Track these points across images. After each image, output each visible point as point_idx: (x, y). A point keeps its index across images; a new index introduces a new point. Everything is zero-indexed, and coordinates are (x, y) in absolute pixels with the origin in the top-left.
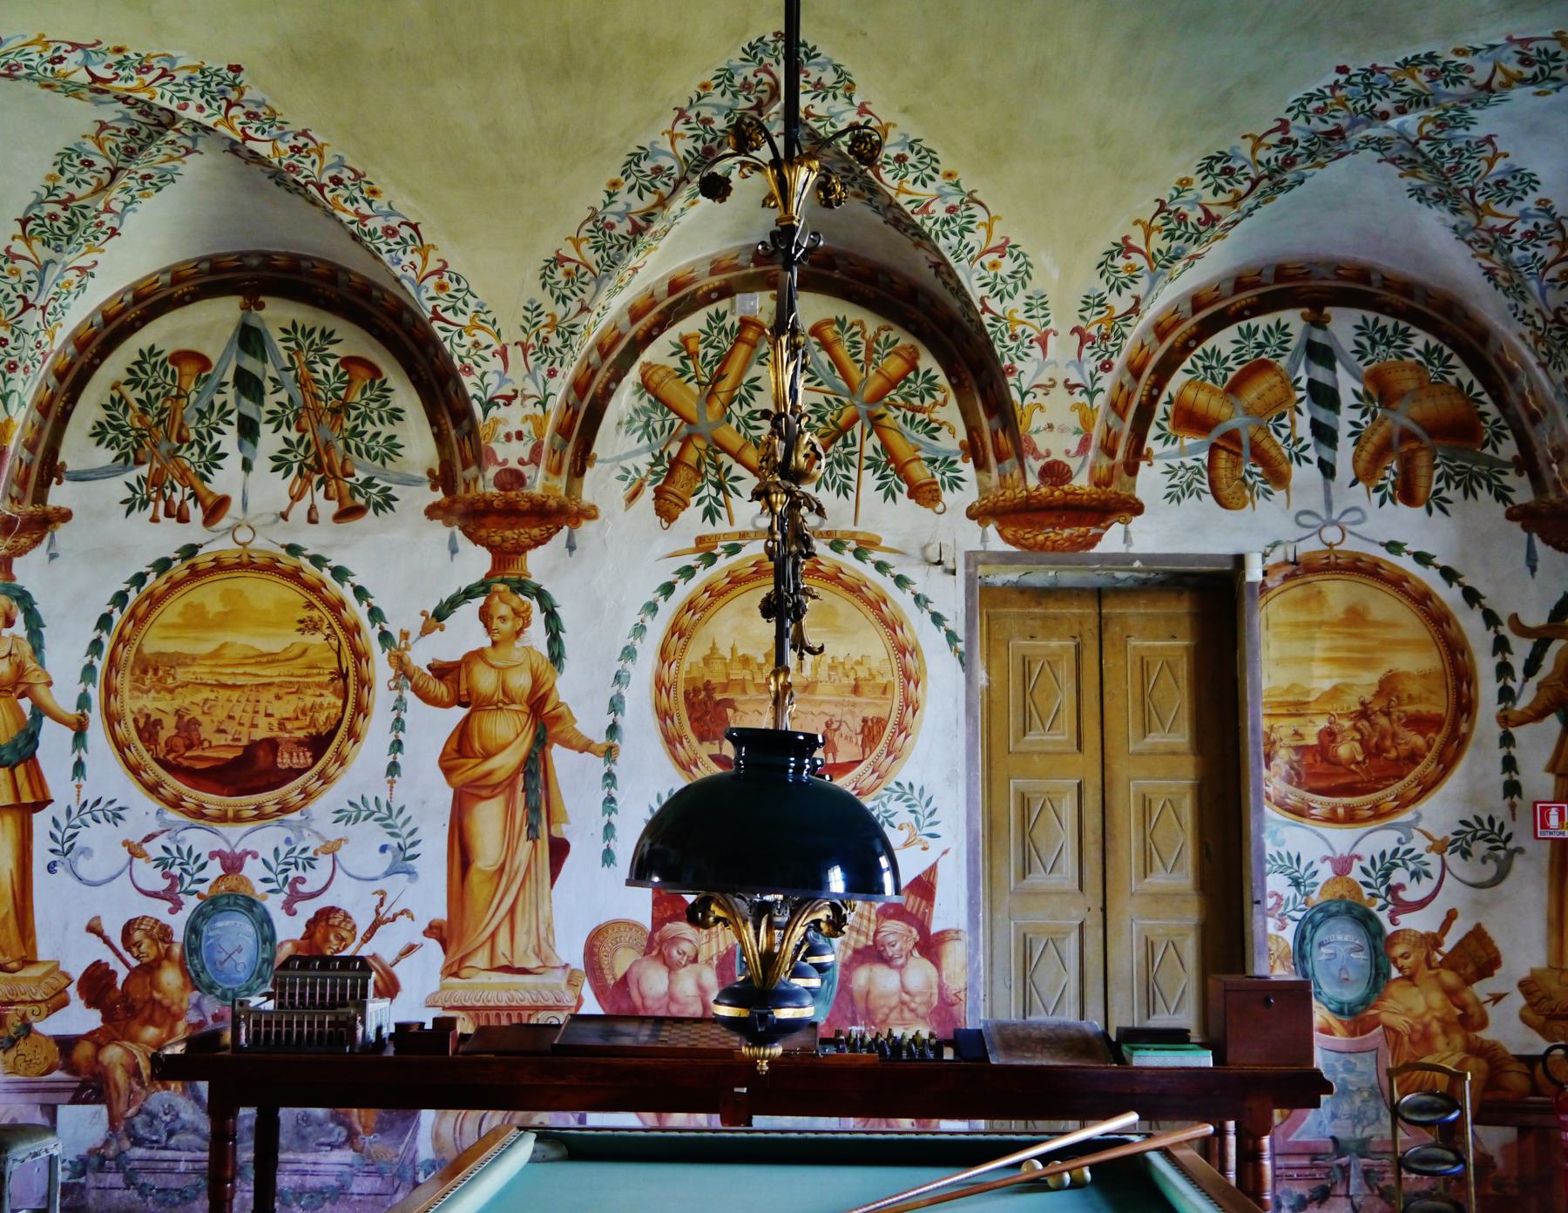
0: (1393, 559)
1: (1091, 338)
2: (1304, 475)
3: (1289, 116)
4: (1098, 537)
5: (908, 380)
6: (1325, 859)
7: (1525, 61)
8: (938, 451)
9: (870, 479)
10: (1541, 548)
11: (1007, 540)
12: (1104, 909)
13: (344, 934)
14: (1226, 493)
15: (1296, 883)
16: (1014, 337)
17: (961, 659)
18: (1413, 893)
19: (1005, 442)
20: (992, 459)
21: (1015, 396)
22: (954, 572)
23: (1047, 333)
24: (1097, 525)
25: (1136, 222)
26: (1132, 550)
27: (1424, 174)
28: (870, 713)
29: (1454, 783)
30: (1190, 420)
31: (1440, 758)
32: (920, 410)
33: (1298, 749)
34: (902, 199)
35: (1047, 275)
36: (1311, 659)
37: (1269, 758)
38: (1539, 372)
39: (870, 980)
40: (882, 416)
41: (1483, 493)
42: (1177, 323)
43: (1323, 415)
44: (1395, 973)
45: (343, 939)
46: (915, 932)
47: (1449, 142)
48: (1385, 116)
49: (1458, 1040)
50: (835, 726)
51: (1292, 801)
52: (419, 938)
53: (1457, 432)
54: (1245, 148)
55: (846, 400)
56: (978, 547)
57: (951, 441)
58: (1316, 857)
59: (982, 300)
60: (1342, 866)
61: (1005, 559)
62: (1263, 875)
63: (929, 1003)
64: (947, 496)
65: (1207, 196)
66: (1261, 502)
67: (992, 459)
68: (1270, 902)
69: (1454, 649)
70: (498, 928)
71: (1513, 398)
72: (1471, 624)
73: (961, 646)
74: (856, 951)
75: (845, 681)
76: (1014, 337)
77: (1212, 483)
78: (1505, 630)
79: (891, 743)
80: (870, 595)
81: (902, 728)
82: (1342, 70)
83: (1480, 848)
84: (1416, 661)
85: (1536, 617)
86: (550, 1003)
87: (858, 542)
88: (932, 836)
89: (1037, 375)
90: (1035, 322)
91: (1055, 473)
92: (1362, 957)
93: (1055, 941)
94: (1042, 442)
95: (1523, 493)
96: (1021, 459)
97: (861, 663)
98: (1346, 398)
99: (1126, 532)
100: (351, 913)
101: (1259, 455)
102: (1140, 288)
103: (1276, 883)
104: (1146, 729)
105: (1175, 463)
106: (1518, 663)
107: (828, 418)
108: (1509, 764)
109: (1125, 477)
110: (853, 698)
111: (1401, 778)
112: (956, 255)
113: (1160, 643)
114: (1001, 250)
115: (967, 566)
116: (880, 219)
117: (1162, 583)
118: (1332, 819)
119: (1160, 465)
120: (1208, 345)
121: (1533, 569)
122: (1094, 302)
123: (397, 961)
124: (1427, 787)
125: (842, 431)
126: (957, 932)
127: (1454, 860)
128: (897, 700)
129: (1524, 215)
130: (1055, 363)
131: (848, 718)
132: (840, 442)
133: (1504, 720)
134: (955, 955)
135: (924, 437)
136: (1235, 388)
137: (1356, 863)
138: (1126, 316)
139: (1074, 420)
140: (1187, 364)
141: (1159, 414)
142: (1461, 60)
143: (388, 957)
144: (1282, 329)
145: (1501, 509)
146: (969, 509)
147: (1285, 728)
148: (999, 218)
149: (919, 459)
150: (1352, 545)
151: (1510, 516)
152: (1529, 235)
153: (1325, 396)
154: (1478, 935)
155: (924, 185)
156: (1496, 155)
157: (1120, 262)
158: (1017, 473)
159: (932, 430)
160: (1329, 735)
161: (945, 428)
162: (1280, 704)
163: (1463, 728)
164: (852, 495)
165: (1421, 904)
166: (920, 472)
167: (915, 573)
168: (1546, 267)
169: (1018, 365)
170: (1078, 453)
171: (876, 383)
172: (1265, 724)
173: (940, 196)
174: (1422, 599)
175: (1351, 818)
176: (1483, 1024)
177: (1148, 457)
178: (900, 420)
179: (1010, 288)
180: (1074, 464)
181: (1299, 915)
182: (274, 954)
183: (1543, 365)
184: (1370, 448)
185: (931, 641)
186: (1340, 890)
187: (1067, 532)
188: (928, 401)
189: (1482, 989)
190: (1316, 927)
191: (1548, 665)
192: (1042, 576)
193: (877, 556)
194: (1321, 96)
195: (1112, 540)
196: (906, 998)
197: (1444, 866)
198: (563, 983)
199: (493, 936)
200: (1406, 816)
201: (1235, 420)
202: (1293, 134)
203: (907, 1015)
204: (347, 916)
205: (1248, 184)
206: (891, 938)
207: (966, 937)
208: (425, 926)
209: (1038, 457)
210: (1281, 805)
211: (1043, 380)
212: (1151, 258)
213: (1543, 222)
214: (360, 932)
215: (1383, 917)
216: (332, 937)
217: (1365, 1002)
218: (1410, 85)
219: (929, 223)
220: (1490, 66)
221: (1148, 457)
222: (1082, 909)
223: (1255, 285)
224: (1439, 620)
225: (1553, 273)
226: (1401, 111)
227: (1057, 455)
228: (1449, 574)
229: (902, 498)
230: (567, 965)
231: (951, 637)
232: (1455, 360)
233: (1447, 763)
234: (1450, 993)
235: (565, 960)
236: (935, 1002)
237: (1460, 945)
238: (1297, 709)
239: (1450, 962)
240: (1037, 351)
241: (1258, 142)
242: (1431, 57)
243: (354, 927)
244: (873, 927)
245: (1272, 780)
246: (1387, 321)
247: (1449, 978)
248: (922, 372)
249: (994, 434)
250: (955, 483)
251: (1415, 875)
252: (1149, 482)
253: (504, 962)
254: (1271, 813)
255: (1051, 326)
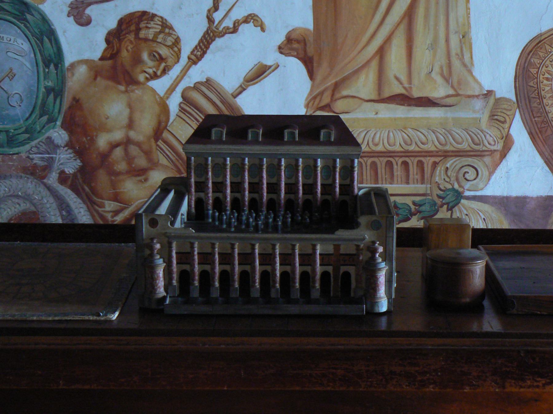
13: (164, 51)
45: (161, 59)
52: (272, 57)
70: (388, 39)
86: (464, 146)
100: (171, 21)
123: (242, 89)
143: (229, 83)
182: (63, 82)
198: (485, 118)
199: (381, 52)
204: (165, 26)
208: (281, 38)
214: (187, 49)
216: (145, 56)
230: (490, 93)
235: (487, 86)
243: (177, 41)
253: (398, 89)
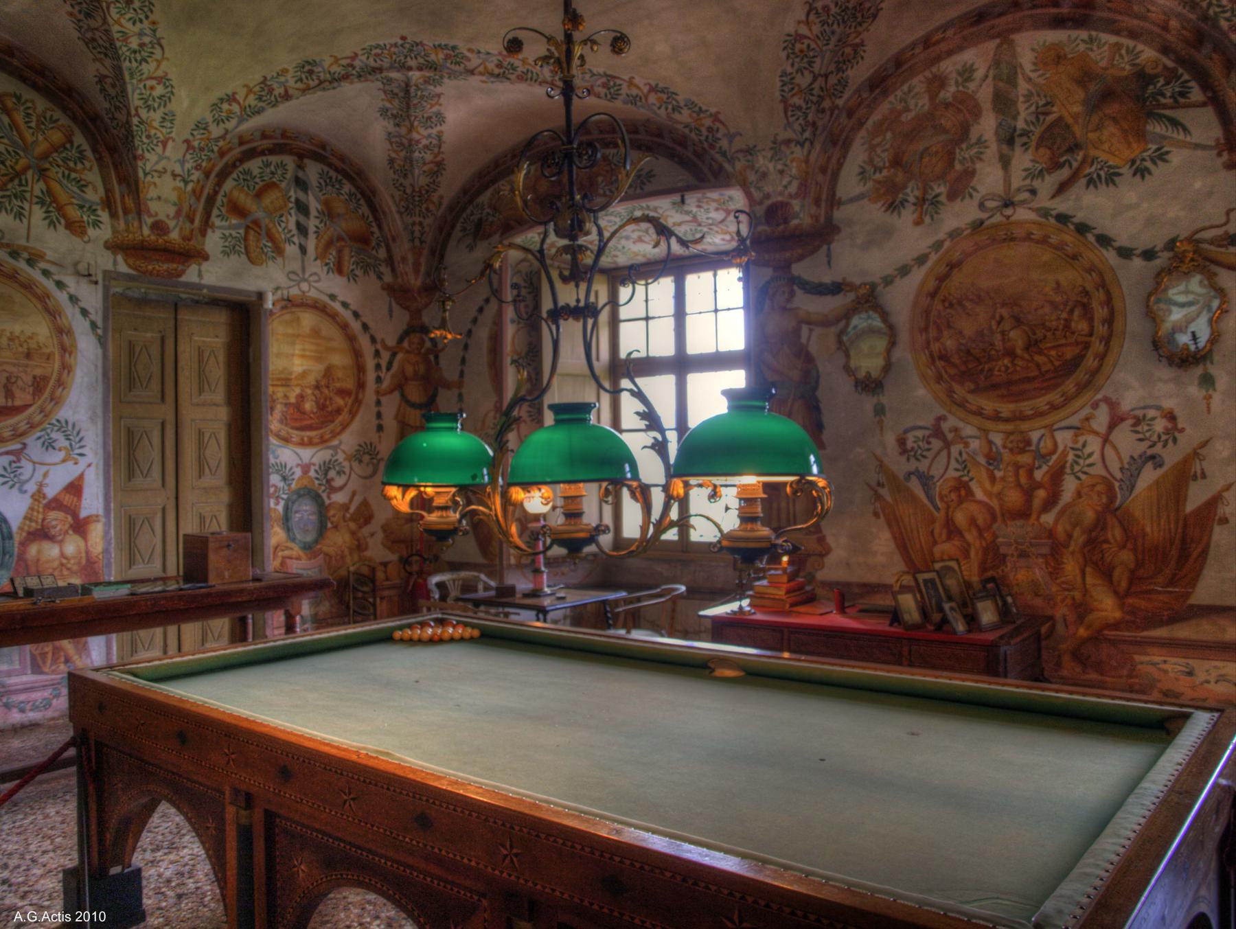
0: (332, 304)
1: (194, 148)
2: (291, 250)
3: (360, 53)
4: (183, 272)
5: (66, 149)
6: (298, 465)
7: (499, 65)
8: (84, 200)
9: (38, 213)
10: (396, 307)
11: (130, 266)
12: (177, 498)
14: (253, 255)
15: (284, 479)
16: (148, 137)
17: (99, 341)
18: (338, 482)
19: (130, 202)
20: (120, 212)
21: (141, 174)
22: (96, 283)
23: (168, 139)
24: (183, 263)
25: (246, 86)
26: (203, 282)
27: (396, 102)
28: (38, 372)
29: (356, 425)
30: (237, 210)
31: (350, 412)
32: (75, 171)
33: (286, 405)
34: (116, 28)
35: (182, 102)
36: (293, 355)
37: (272, 409)
38: (397, 216)
39: (39, 552)
40: (46, 170)
41: (372, 274)
42: (230, 149)
43: (302, 219)
44: (329, 525)
46: (70, 518)
47: (423, 90)
48: (410, 69)
49: (356, 557)
50: (13, 380)
51: (283, 433)
53: (362, 240)
54: (327, 61)
55: (21, 153)
56: (110, 267)
57: (94, 195)
58: (294, 464)
59: (136, 110)
60: (306, 468)
61: (129, 278)
62: (269, 474)
63: (79, 563)
64: (91, 232)
65: (291, 83)
66: (270, 263)
67: (120, 212)
68: (272, 490)
69: (357, 354)
71: (386, 228)
72: (364, 342)
73: (100, 332)
74: (29, 533)
75: (20, 349)
76: (148, 137)
77: (246, 248)
78: (379, 346)
79: (53, 393)
80: (39, 292)
81: (60, 383)
82: (403, 38)
83: (366, 458)
84: (340, 360)
85: (391, 341)
87: (30, 254)
88: (82, 455)
89: (157, 163)
90: (164, 130)
91: (159, 227)
92: (313, 518)
93: (149, 520)
94: (154, 206)
95: (388, 278)
96: (139, 213)
97: (31, 338)
98: (313, 212)
99: (200, 271)
101: (270, 237)
102: (230, 125)
103: (275, 479)
104: (201, 391)
105: (227, 232)
106: (384, 364)
107: (8, 163)
108: (379, 415)
109: (200, 238)
110: (26, 362)
111: (333, 421)
112: (131, 75)
113: (208, 337)
114: (160, 80)
115: (104, 280)
116: (76, 34)
117: (206, 303)
118: (302, 444)
119: (218, 233)
120: (247, 166)
121: (391, 316)
122: (201, 126)
124: (345, 427)
125: (18, 175)
126: (97, 516)
127: (355, 464)
128: (57, 365)
129: (430, 136)
130: (168, 159)
131: (22, 375)
132: (16, 182)
133: (377, 393)
134: (96, 532)
135: (75, 189)
136: (259, 195)
137: (313, 468)
138: (217, 140)
139: (173, 197)
140: (234, 175)
141: (219, 203)
142: (468, 54)
144: (283, 166)
145: (378, 284)
146: (106, 242)
147: (280, 392)
148: (168, 59)
149: (72, 204)
150: (313, 294)
151: (383, 289)
152: (426, 147)
153: (302, 208)
154: (365, 503)
155: (134, 23)
156: (437, 103)
157: (225, 106)
158: (136, 224)
159: (82, 186)
160: (301, 397)
161: (90, 187)
162: (278, 379)
163: (360, 396)
164: (25, 221)
165: (341, 488)
166: (74, 213)
167: (70, 281)
168: (425, 164)
169: (147, 155)
170: (174, 218)
171: (43, 147)
172: (271, 389)
173: (141, 34)
174: (344, 327)
175: (310, 443)
176: (366, 548)
177: (213, 227)
178: (60, 175)
179: (156, 105)
180: (172, 224)
181: (285, 497)
183: (400, 213)
184: (323, 241)
185: (80, 326)
186: (305, 482)
187: (165, 266)
188: (79, 166)
189: (366, 531)
190: (293, 503)
191: (396, 365)
192: (138, 290)
193: (43, 265)
194: (384, 47)
195: (191, 275)
196: (64, 561)
197: (351, 468)
200: (335, 442)
201: (260, 214)
202: (357, 63)
203: (65, 572)
205: (317, 82)
206: (54, 523)
207: (103, 520)
209: (150, 216)
210: (278, 436)
211: (159, 167)
212: (243, 109)
213: (435, 142)
215: (324, 496)
217: (316, 541)
218: (433, 57)
219: (124, 49)
220: (479, 61)
221: (213, 227)
222: (164, 498)
223: (271, 137)
224: (351, 339)
225: (425, 168)
226: (420, 69)
227: (162, 217)
228: (356, 315)
229: (61, 228)
231: (94, 325)
232: (362, 202)
233: (353, 414)
234: (353, 533)
236: (84, 561)
237: (358, 509)
238: (286, 382)
239: (353, 519)
240: (159, 149)
241: (337, 60)
242: (454, 48)
244: (41, 516)
245: (274, 422)
246: (333, 174)
247: (353, 526)
248: (76, 145)
249: (123, 197)
250: (97, 224)
251: (338, 473)
252: (213, 242)
254: (273, 441)
255: (173, 135)
